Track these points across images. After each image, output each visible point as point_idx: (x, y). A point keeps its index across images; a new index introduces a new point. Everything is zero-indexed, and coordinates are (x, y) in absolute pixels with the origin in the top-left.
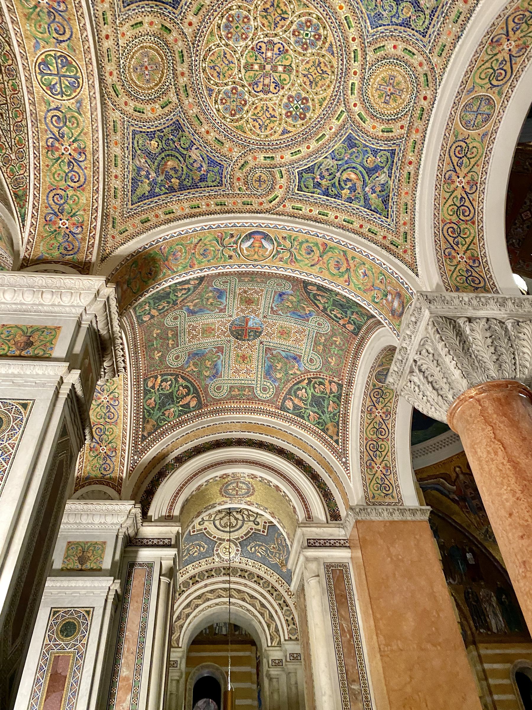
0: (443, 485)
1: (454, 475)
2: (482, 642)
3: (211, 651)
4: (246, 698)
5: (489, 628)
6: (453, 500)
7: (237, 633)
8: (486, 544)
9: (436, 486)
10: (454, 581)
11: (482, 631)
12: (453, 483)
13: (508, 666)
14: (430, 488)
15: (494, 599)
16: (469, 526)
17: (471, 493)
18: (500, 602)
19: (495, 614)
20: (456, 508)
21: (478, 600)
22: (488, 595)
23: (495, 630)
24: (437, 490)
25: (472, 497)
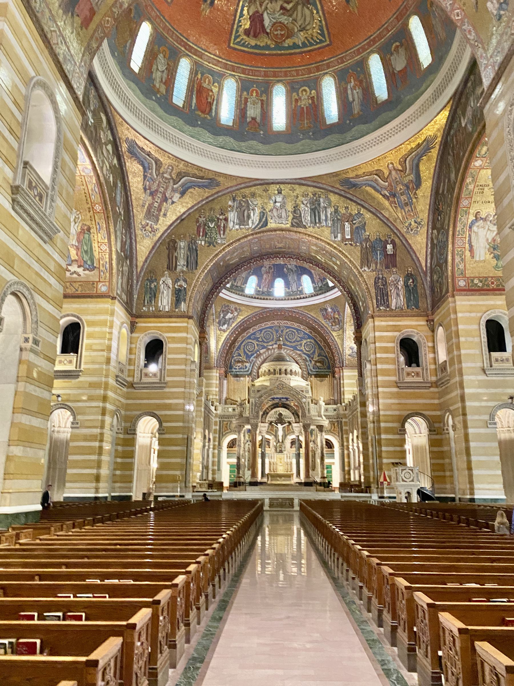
0: (376, 180)
1: (386, 173)
2: (380, 316)
3: (154, 322)
4: (181, 353)
5: (388, 306)
6: (384, 196)
7: (177, 310)
8: (407, 236)
9: (370, 183)
10: (369, 268)
11: (381, 308)
12: (385, 180)
13: (397, 334)
14: (365, 184)
15: (401, 283)
16: (395, 221)
17: (401, 189)
18: (406, 285)
19: (398, 295)
20: (386, 203)
21: (385, 284)
22: (396, 280)
23: (393, 308)
24: (371, 186)
25: (401, 193)
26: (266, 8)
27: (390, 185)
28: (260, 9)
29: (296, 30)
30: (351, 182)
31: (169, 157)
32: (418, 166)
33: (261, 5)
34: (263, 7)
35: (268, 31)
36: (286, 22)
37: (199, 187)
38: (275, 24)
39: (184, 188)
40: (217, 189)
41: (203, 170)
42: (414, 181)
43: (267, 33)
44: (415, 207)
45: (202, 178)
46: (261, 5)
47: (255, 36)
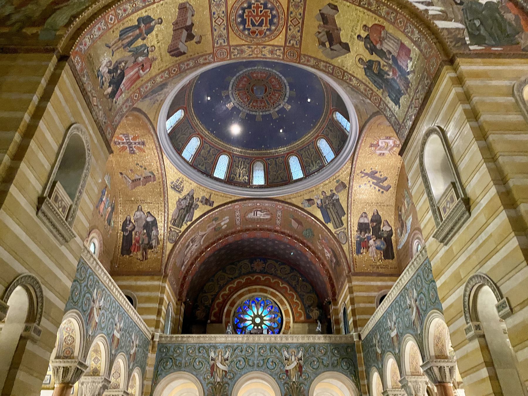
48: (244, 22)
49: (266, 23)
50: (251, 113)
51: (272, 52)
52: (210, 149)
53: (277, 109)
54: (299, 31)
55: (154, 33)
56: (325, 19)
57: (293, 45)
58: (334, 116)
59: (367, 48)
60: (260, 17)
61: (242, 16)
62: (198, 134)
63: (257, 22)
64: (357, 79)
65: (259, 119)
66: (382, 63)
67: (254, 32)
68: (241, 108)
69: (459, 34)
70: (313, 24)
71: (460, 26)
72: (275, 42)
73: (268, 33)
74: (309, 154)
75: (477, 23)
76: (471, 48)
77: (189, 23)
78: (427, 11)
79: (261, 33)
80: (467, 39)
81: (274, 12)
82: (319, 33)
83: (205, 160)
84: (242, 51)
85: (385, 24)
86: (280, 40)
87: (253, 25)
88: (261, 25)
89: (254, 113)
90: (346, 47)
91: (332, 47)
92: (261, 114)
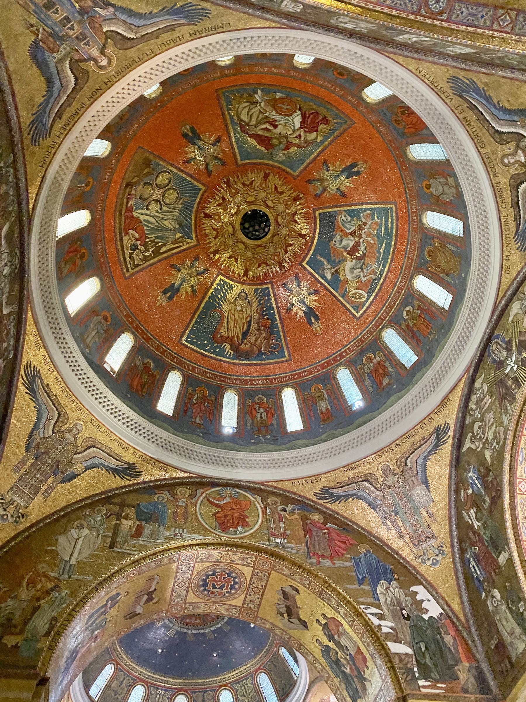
0: (129, 27)
9: (142, 22)
17: (72, 28)
25: (69, 21)
26: (294, 131)
27: (96, 28)
28: (302, 134)
29: (262, 104)
30: (185, 17)
31: (495, 176)
32: (49, 82)
33: (300, 136)
34: (298, 133)
35: (298, 112)
36: (274, 113)
37: (489, 99)
38: (288, 116)
39: (515, 118)
40: (461, 75)
41: (461, 117)
42: (47, 54)
43: (300, 109)
44: (25, 7)
45: (473, 108)
46: (300, 136)
47: (317, 114)
48: (205, 585)
49: (227, 587)
50: (182, 630)
51: (227, 610)
52: (124, 679)
53: (213, 629)
54: (258, 598)
55: (117, 605)
56: (285, 595)
57: (251, 607)
58: (280, 651)
59: (325, 634)
60: (222, 582)
61: (204, 581)
62: (115, 660)
63: (218, 585)
64: (314, 657)
65: (189, 638)
66: (339, 653)
67: (213, 593)
68: (171, 625)
69: (408, 662)
70: (272, 596)
71: (410, 651)
72: (233, 602)
73: (227, 595)
74: (246, 691)
75: (423, 646)
76: (421, 683)
77: (152, 589)
78: (380, 626)
79: (220, 594)
80: (416, 669)
81: (237, 580)
82: (279, 604)
83: (115, 695)
84: (198, 607)
85: (344, 623)
86: (238, 601)
87: (214, 587)
88: (222, 588)
89: (185, 631)
90: (305, 625)
91: (290, 620)
92: (193, 632)
